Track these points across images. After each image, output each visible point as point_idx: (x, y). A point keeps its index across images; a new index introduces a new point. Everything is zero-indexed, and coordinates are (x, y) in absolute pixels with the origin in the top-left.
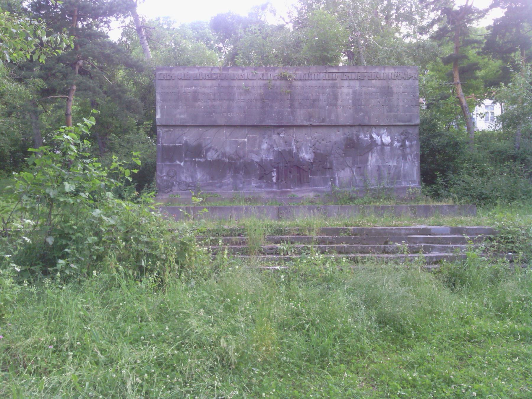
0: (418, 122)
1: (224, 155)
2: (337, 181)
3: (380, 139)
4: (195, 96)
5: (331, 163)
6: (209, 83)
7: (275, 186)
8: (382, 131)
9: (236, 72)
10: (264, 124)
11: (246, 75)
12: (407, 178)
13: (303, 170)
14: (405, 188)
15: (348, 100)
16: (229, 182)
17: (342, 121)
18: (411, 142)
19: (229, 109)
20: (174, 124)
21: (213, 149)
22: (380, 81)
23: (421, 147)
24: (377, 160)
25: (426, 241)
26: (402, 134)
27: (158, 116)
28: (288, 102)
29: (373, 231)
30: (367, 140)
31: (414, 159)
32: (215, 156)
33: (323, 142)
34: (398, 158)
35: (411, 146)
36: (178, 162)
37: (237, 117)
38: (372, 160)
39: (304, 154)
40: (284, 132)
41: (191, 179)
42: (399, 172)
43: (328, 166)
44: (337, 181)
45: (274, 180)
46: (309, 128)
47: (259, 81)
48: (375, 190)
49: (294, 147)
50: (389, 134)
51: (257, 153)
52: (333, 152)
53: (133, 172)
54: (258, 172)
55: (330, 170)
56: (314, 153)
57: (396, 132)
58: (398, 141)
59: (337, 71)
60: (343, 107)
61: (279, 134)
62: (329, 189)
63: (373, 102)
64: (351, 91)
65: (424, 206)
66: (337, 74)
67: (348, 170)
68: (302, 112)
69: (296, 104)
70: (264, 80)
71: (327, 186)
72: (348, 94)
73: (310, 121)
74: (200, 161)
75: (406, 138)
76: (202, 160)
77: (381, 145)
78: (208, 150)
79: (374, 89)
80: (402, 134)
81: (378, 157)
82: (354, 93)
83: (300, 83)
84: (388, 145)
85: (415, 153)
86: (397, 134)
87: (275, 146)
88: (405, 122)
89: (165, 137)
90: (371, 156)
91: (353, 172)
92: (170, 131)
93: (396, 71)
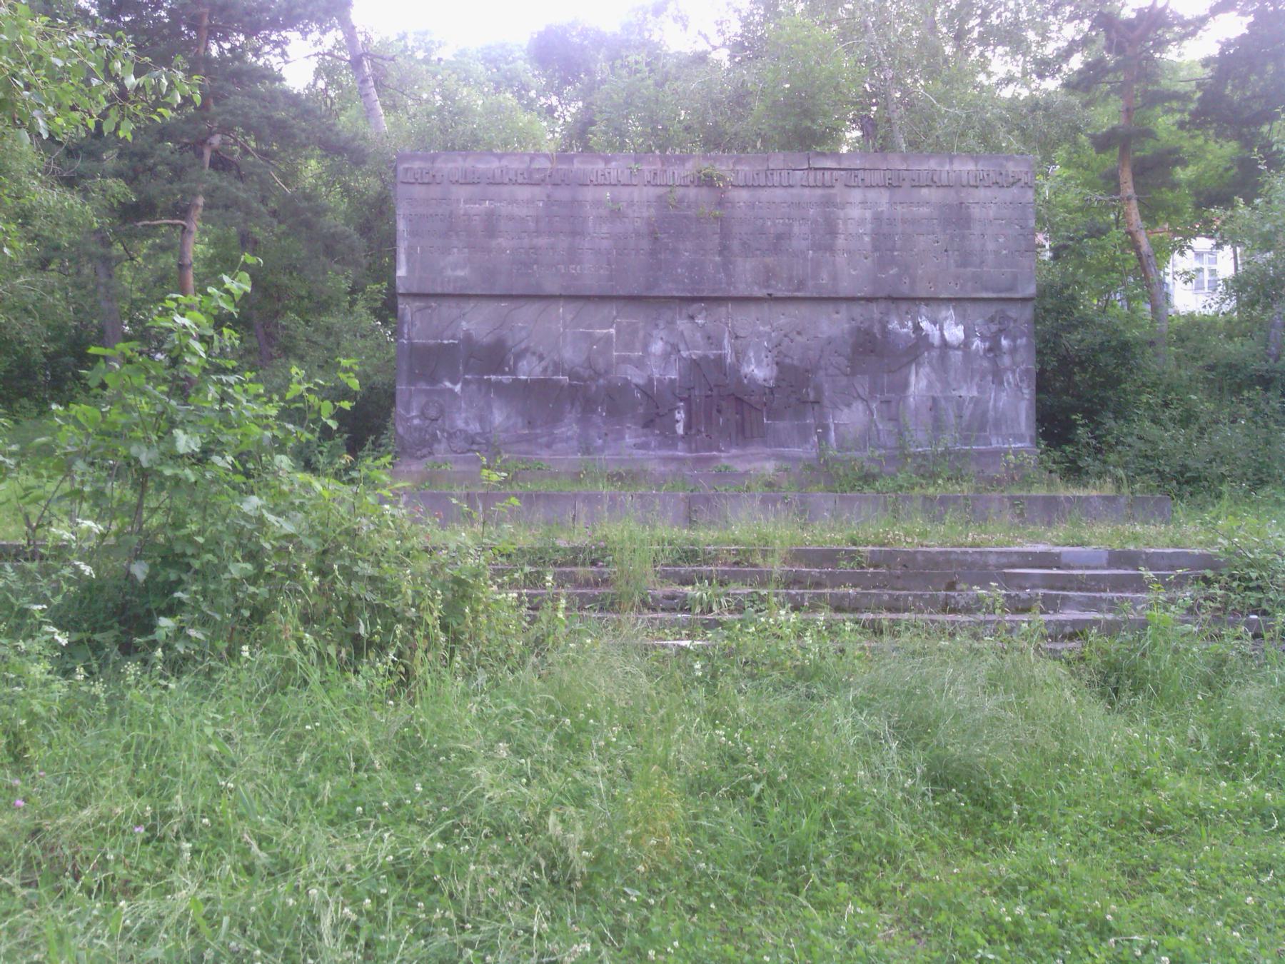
0: (1031, 290)
1: (558, 367)
2: (833, 434)
3: (937, 333)
4: (491, 224)
5: (819, 390)
6: (524, 193)
7: (680, 445)
8: (944, 313)
9: (589, 167)
10: (655, 293)
11: (614, 173)
13: (751, 406)
14: (997, 453)
15: (860, 236)
16: (569, 433)
17: (845, 288)
18: (1014, 340)
19: (573, 256)
20: (439, 290)
21: (534, 353)
22: (941, 191)
23: (1039, 352)
24: (930, 385)
25: (1050, 582)
26: (992, 320)
27: (401, 272)
28: (716, 239)
29: (920, 557)
30: (907, 334)
31: (1022, 381)
32: (538, 369)
33: (799, 338)
34: (983, 378)
35: (1014, 350)
36: (448, 384)
37: (591, 275)
38: (917, 382)
39: (752, 367)
40: (704, 313)
41: (478, 425)
42: (985, 413)
43: (812, 396)
44: (833, 434)
45: (680, 429)
46: (766, 306)
47: (645, 189)
48: (924, 456)
49: (728, 350)
50: (962, 319)
51: (640, 364)
52: (822, 363)
53: (340, 408)
54: (641, 410)
55: (816, 407)
56: (777, 364)
57: (978, 315)
58: (983, 338)
59: (834, 165)
60: (849, 252)
61: (692, 318)
62: (814, 453)
63: (922, 242)
64: (868, 214)
65: (1044, 497)
66: (835, 173)
67: (859, 406)
68: (748, 266)
69: (735, 245)
70: (656, 185)
71: (808, 446)
72: (862, 222)
73: (768, 287)
74: (499, 383)
75: (1001, 331)
76: (506, 379)
77: (940, 347)
78: (520, 356)
79: (924, 210)
80: (992, 320)
81: (933, 376)
82: (877, 218)
83: (744, 194)
84: (958, 348)
85: (1023, 367)
86: (979, 321)
87: (682, 347)
88: (1000, 291)
89: (418, 324)
90: (917, 373)
91: (872, 414)
92: (430, 307)
93: (980, 167)
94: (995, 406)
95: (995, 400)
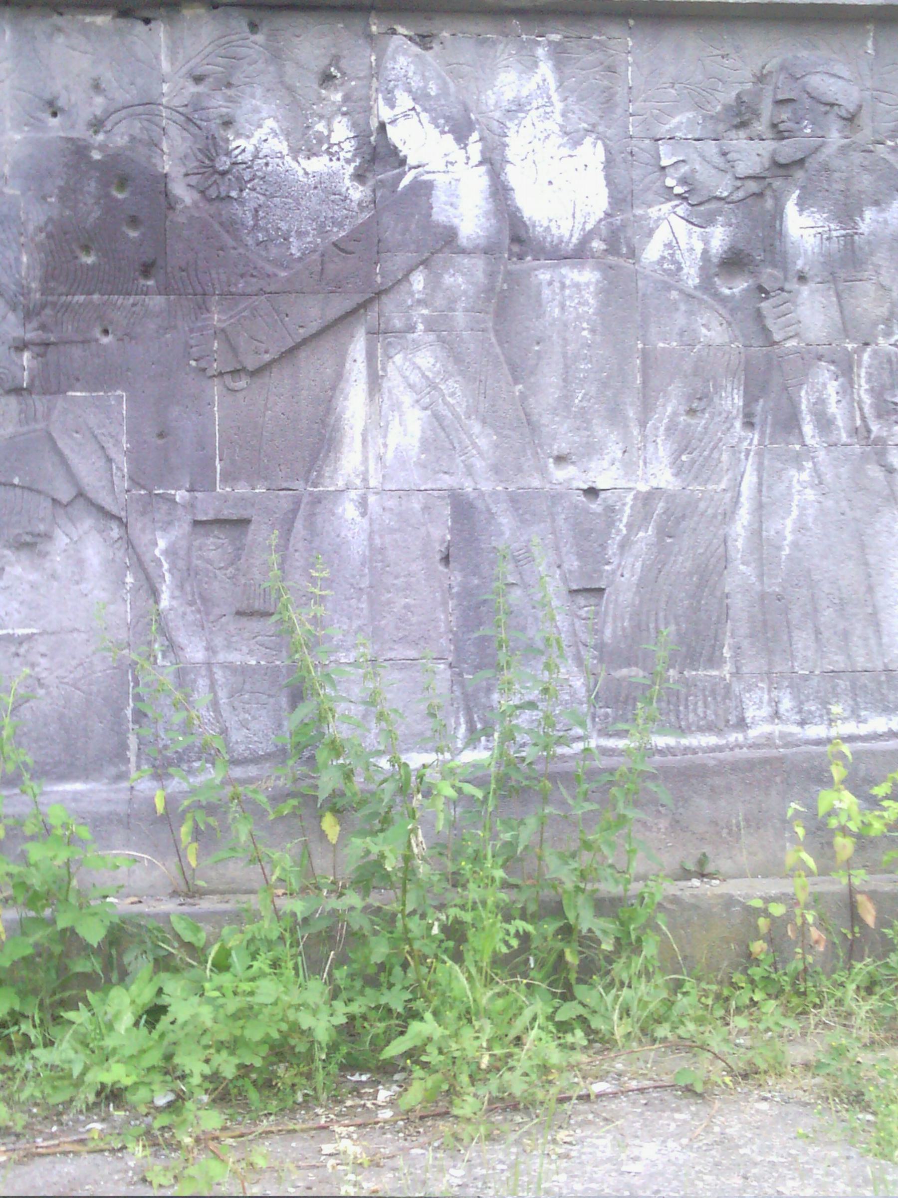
12: (803, 640)
77: (489, 250)
90: (375, 382)
94: (757, 533)
95: (759, 509)
